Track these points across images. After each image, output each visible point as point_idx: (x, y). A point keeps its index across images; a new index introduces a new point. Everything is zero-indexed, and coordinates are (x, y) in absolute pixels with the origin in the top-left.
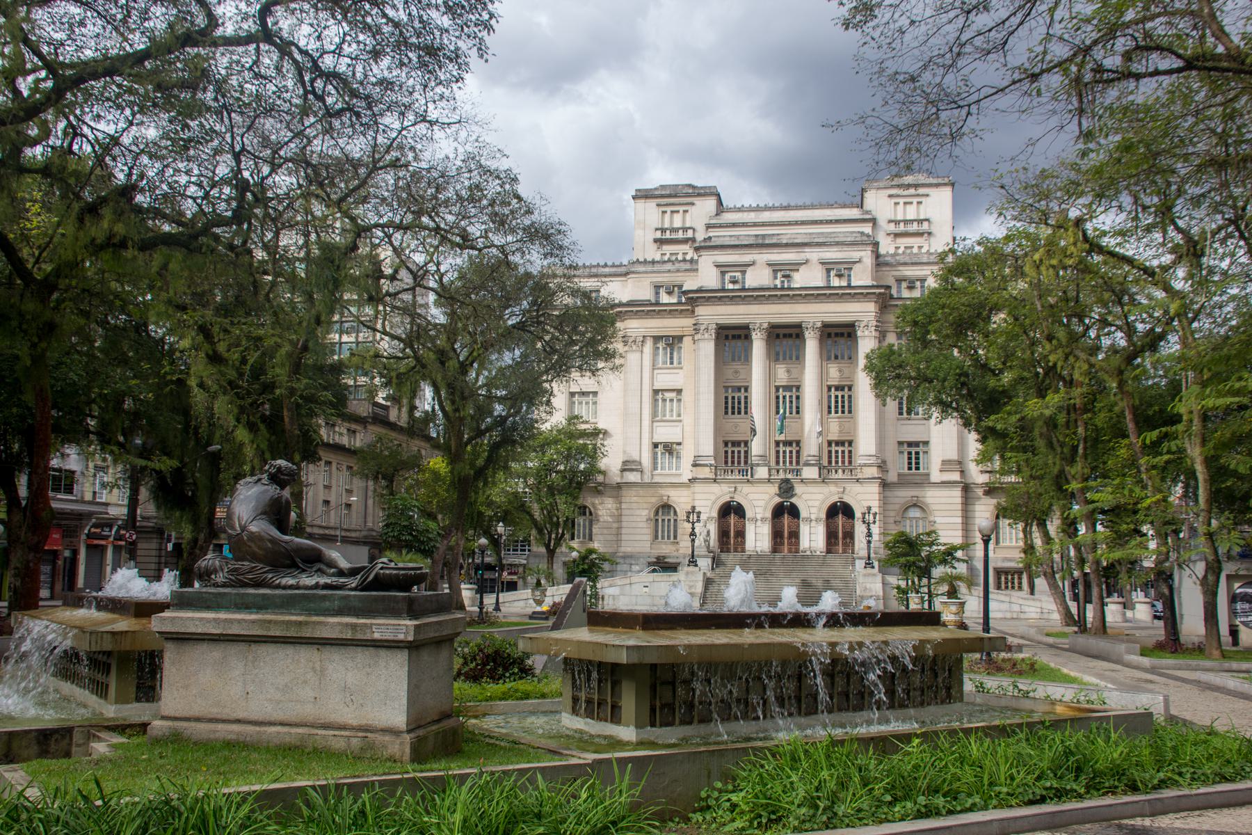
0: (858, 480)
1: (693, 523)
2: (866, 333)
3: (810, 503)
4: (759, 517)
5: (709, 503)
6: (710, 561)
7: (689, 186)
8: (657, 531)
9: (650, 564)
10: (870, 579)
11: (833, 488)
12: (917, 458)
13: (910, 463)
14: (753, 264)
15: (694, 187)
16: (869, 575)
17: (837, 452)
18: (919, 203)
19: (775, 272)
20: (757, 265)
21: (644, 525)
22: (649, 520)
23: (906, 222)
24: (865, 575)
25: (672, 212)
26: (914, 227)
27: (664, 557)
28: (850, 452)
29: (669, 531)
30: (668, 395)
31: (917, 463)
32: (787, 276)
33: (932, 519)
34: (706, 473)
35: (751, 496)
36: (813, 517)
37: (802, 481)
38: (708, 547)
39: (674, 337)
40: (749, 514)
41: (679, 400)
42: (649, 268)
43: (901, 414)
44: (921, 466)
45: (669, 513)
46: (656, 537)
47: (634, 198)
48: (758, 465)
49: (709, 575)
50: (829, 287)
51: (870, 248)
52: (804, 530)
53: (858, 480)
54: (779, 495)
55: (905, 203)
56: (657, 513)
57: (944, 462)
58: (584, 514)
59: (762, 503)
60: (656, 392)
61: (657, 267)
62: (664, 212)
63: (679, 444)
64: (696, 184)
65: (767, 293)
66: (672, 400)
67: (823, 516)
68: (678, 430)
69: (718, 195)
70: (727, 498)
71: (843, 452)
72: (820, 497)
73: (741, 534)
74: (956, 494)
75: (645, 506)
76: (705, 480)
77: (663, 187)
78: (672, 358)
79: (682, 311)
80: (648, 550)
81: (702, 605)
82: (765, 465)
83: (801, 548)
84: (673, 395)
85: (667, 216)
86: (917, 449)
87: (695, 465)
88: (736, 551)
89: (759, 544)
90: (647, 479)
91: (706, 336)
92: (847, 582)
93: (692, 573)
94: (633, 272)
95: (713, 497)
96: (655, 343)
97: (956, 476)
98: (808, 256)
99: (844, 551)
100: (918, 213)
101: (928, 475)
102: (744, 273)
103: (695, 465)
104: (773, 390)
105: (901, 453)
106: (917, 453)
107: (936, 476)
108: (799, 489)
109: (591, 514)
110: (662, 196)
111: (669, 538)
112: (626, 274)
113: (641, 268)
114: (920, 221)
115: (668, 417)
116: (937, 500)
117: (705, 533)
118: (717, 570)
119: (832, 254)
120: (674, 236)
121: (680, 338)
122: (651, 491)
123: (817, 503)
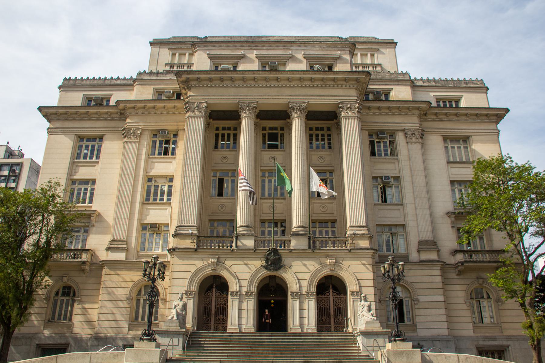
5: (189, 275)
22: (129, 298)
34: (188, 243)
42: (154, 77)
47: (151, 43)
52: (293, 305)
54: (266, 267)
57: (421, 243)
58: (68, 295)
61: (161, 77)
64: (200, 36)
70: (209, 271)
73: (223, 311)
74: (436, 273)
77: (174, 37)
88: (217, 329)
91: (197, 113)
95: (193, 269)
97: (433, 256)
104: (260, 174)
107: (414, 256)
108: (286, 261)
109: (74, 294)
116: (418, 279)
119: (315, 52)
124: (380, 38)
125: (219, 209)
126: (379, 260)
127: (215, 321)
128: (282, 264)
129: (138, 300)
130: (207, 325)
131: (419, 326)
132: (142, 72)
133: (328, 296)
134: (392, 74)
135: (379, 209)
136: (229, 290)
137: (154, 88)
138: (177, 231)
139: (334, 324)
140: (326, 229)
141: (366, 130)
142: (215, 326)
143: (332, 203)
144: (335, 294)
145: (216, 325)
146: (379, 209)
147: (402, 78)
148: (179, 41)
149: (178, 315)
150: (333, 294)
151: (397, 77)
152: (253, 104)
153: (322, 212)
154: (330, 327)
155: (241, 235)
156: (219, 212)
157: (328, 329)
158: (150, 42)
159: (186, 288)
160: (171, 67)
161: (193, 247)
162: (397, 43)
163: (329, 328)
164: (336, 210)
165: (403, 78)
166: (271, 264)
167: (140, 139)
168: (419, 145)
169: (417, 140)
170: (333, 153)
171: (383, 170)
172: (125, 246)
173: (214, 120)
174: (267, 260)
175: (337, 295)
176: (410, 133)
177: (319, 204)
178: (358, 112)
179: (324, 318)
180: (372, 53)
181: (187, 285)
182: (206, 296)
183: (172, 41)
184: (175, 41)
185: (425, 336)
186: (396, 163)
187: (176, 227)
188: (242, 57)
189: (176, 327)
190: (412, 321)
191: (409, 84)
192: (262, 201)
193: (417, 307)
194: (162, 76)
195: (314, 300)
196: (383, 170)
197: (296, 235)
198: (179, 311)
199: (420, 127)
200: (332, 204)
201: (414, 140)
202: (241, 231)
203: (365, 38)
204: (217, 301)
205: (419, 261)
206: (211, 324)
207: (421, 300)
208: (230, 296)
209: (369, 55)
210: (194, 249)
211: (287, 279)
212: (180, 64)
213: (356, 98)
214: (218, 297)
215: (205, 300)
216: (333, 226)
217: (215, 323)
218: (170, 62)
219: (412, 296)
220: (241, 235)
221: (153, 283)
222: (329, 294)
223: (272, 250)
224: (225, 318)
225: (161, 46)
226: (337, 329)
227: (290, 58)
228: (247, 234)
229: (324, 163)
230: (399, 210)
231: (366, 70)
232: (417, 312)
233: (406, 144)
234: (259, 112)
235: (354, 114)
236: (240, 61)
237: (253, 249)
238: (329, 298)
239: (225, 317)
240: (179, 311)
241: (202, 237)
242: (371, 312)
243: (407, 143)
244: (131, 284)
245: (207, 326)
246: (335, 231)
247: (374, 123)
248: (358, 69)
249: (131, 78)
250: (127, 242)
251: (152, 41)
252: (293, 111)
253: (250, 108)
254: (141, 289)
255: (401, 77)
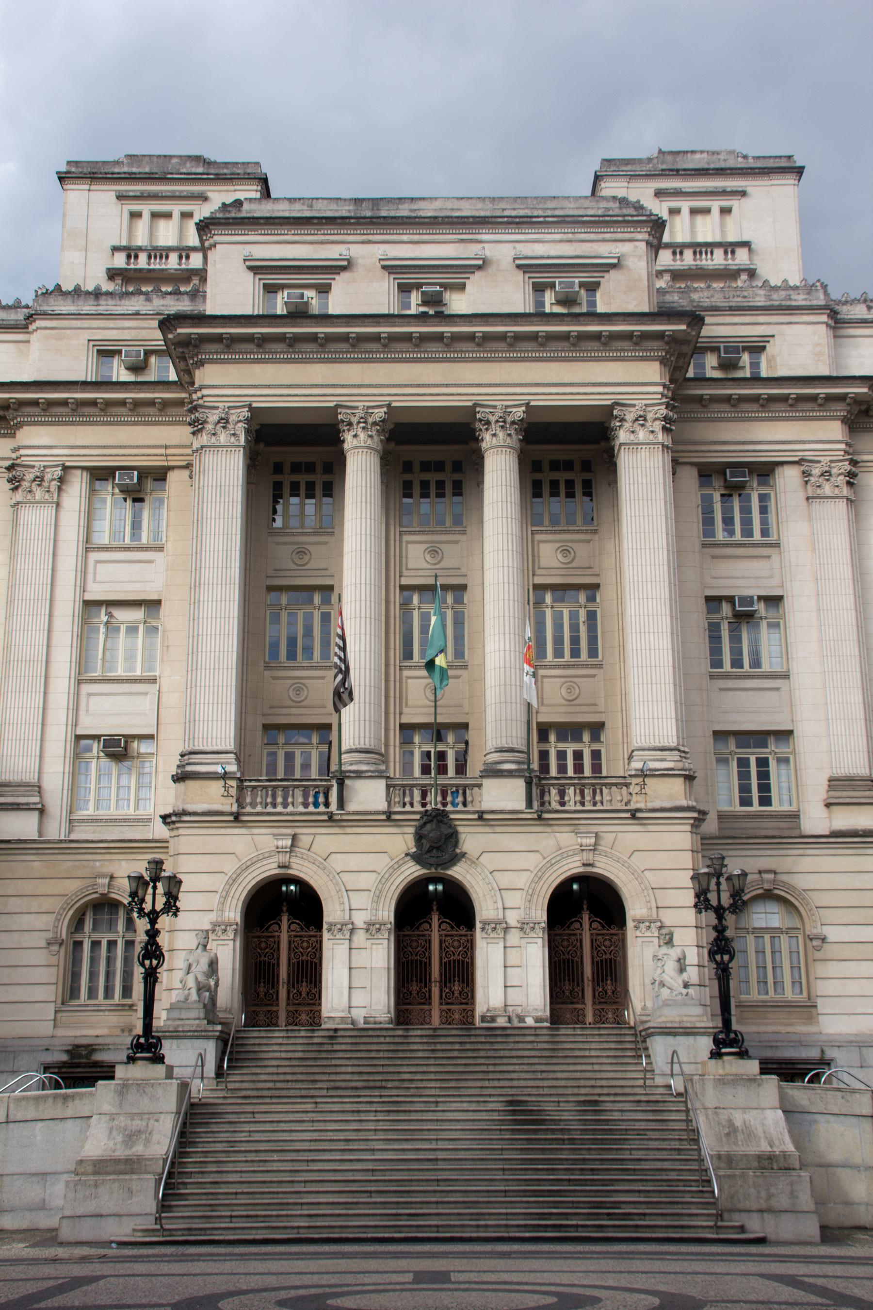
0: (634, 814)
1: (153, 917)
2: (642, 435)
3: (505, 880)
4: (360, 919)
5: (218, 883)
6: (210, 1049)
7: (198, 159)
8: (75, 976)
9: (47, 1068)
10: (741, 1096)
11: (565, 838)
12: (764, 775)
13: (745, 789)
14: (345, 266)
15: (207, 163)
16: (737, 1080)
17: (562, 755)
18: (726, 211)
19: (404, 289)
20: (358, 272)
21: (40, 957)
23: (699, 248)
24: (722, 1082)
25: (155, 215)
26: (718, 259)
27: (91, 1049)
28: (596, 755)
29: (109, 975)
30: (123, 615)
31: (765, 788)
32: (433, 300)
33: (813, 929)
35: (339, 862)
36: (513, 918)
37: (481, 816)
38: (210, 1008)
39: (144, 473)
40: (332, 912)
41: (152, 630)
42: (88, 307)
43: (717, 663)
44: (774, 794)
45: (111, 926)
46: (73, 992)
47: (63, 178)
48: (359, 775)
49: (199, 1089)
50: (541, 316)
51: (643, 235)
53: (634, 814)
54: (417, 858)
55: (694, 212)
56: (78, 923)
57: (835, 783)
59: (368, 881)
60: (90, 605)
62: (135, 215)
63: (150, 737)
65: (384, 330)
66: (132, 630)
67: (541, 915)
68: (147, 704)
69: (264, 181)
70: (269, 869)
71: (578, 755)
72: (532, 861)
75: (47, 904)
76: (210, 818)
78: (136, 526)
79: (166, 404)
80: (46, 1029)
81: (164, 1206)
82: (380, 775)
83: (480, 1008)
84: (137, 615)
85: (142, 226)
86: (762, 752)
87: (180, 778)
88: (293, 1020)
89: (359, 999)
90: (55, 830)
91: (223, 437)
92: (654, 1105)
93: (142, 1086)
94: (45, 315)
95: (230, 866)
96: (92, 491)
98: (489, 251)
99: (600, 1018)
100: (723, 232)
101: (795, 816)
102: (324, 290)
103: (180, 778)
104: (396, 597)
105: (723, 761)
106: (763, 763)
110: (131, 178)
111: (108, 992)
112: (23, 327)
113: (65, 307)
114: (730, 248)
115: (120, 672)
116: (823, 882)
117: (204, 965)
118: (235, 1079)
120: (156, 265)
121: (160, 475)
122: (66, 863)
123: (523, 880)
124: (751, 153)
125: (292, 696)
126: (720, 829)
127: (288, 998)
128: (458, 851)
129: (78, 945)
130: (269, 1008)
131: (823, 1006)
132: (51, 288)
133: (578, 931)
134: (775, 289)
135: (721, 689)
136: (325, 919)
137: (89, 340)
138: (184, 766)
139: (594, 1003)
140: (576, 746)
141: (692, 464)
142: (288, 1012)
143: (594, 676)
144: (595, 925)
145: (291, 1008)
146: (721, 689)
147: (804, 303)
148: (147, 170)
149: (200, 989)
150: (590, 925)
151: (790, 299)
152: (376, 411)
153: (566, 700)
154: (583, 1009)
155: (352, 775)
156: (290, 703)
157: (578, 1019)
158: (58, 173)
159: (212, 917)
160: (129, 257)
161: (227, 808)
162: (803, 168)
163: (581, 1012)
164: (603, 695)
165: (808, 303)
166: (430, 850)
167: (59, 495)
168: (842, 505)
169: (837, 491)
170: (596, 537)
171: (738, 578)
172: (36, 799)
173: (267, 444)
174: (419, 838)
175: (600, 928)
176: (816, 472)
177: (558, 680)
178: (664, 428)
179: (567, 987)
180: (726, 204)
181: (215, 908)
182: (265, 934)
183: (126, 169)
184: (134, 170)
185: (840, 1034)
186: (775, 557)
187: (182, 756)
188: (344, 268)
189: (197, 1022)
190: (805, 994)
191: (824, 318)
192: (406, 673)
193: (818, 955)
194: (111, 302)
195: (540, 941)
196: (738, 578)
197: (493, 772)
198: (201, 978)
199: (845, 452)
200: (592, 679)
201: (827, 490)
202: (351, 764)
203: (705, 155)
204: (292, 946)
205: (827, 833)
206: (277, 1005)
207: (831, 938)
208: (326, 935)
209: (716, 211)
210: (231, 814)
211: (472, 887)
212: (155, 249)
213: (660, 389)
214: (296, 936)
215: (263, 945)
216: (596, 737)
217: (288, 1004)
218: (124, 243)
219: (807, 927)
220: (352, 775)
221: (153, 922)
222: (581, 925)
223: (434, 814)
224: (313, 991)
225: (93, 187)
226: (600, 1018)
227: (479, 267)
228: (367, 771)
229: (573, 565)
230: (777, 689)
231: (704, 262)
232: (820, 970)
233: (804, 503)
234: (392, 426)
235: (651, 437)
236: (337, 277)
237: (384, 813)
238: (581, 935)
239: (315, 986)
240: (201, 978)
241: (250, 780)
242: (685, 975)
243: (808, 499)
244: (56, 904)
245: (269, 1011)
246: (600, 751)
247: (715, 443)
248: (682, 260)
249: (17, 305)
250: (39, 787)
251: (63, 168)
252: (487, 429)
253: (370, 420)
254: (84, 914)
255: (802, 297)
